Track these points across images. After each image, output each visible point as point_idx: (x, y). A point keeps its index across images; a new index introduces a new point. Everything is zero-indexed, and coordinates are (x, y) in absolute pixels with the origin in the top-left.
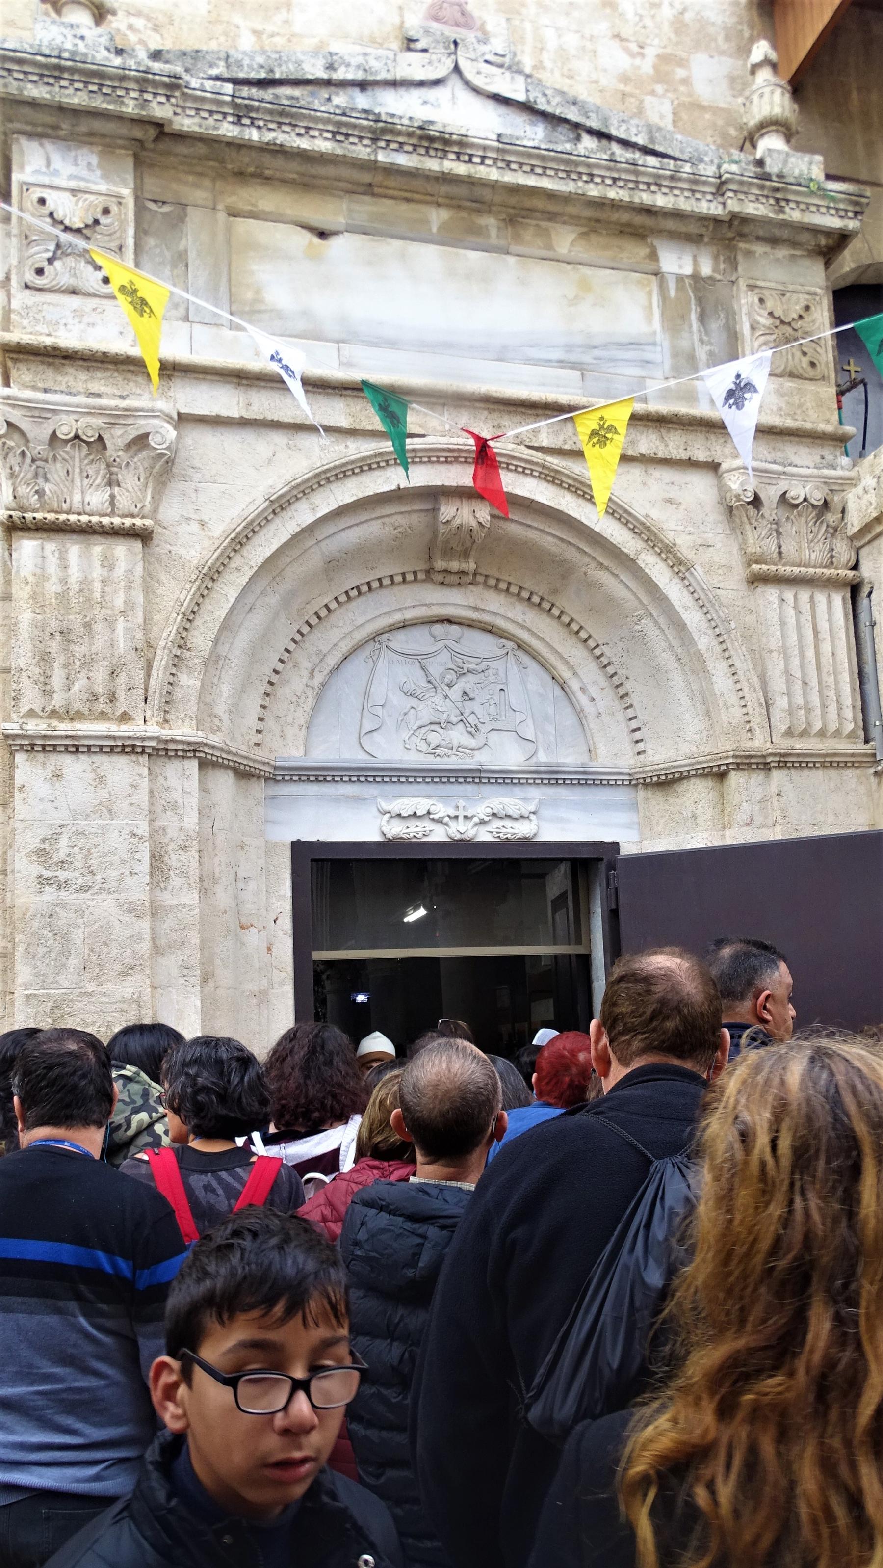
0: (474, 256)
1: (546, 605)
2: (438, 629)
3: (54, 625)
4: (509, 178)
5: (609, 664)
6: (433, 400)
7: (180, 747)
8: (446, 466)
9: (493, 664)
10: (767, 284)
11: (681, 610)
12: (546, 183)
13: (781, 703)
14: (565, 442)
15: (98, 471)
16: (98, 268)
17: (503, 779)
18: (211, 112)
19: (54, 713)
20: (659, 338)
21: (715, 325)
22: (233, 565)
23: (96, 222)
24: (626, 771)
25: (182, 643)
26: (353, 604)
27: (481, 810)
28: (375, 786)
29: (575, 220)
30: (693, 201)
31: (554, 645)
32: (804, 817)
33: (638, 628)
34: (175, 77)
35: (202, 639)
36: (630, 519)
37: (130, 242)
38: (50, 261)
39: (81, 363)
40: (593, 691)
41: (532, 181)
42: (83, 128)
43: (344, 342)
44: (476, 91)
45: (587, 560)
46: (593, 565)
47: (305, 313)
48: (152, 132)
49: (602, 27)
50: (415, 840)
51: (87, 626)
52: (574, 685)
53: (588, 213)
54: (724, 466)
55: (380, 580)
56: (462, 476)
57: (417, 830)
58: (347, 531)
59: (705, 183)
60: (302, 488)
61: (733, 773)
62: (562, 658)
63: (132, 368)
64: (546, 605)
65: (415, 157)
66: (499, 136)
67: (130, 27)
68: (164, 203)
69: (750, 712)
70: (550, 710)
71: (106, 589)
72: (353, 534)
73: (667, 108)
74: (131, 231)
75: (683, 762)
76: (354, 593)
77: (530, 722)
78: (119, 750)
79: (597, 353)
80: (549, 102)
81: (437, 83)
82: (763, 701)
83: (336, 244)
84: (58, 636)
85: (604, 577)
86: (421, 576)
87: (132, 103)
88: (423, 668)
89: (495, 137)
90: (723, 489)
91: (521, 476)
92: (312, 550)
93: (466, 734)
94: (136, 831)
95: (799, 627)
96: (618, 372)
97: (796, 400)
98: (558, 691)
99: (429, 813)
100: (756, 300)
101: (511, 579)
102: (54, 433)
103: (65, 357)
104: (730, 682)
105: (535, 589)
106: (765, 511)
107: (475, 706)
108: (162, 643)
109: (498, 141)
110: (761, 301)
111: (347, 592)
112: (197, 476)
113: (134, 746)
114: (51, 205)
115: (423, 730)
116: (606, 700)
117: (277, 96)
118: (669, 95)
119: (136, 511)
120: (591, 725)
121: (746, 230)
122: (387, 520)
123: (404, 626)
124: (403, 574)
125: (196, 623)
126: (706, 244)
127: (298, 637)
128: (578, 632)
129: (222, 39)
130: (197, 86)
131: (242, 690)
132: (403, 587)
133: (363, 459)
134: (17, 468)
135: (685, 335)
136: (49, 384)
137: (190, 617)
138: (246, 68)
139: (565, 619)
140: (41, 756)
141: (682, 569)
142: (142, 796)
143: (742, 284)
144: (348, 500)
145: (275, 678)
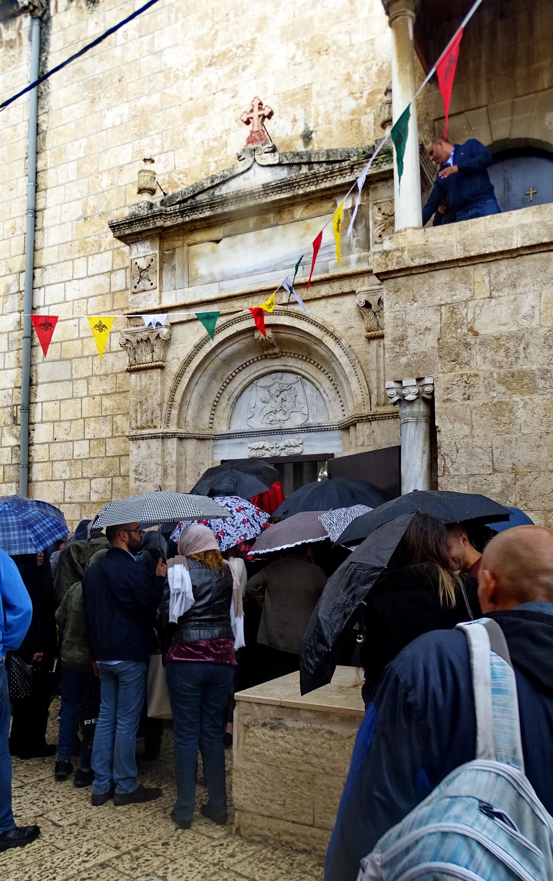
0: (266, 231)
2: (274, 375)
3: (138, 401)
9: (293, 386)
10: (383, 200)
13: (375, 392)
15: (149, 349)
16: (150, 281)
17: (290, 432)
19: (138, 428)
27: (282, 445)
29: (301, 203)
30: (342, 179)
32: (383, 441)
35: (178, 397)
37: (158, 269)
38: (138, 283)
40: (328, 391)
42: (144, 236)
47: (211, 274)
48: (161, 231)
49: (345, 92)
52: (321, 390)
53: (304, 199)
56: (251, 323)
59: (345, 169)
65: (237, 205)
67: (179, 179)
70: (315, 401)
72: (229, 350)
74: (158, 265)
76: (241, 368)
77: (306, 407)
81: (248, 169)
83: (221, 243)
85: (316, 347)
87: (151, 224)
88: (269, 391)
100: (377, 209)
104: (358, 385)
106: (373, 307)
110: (380, 209)
112: (177, 343)
116: (332, 394)
118: (373, 111)
123: (262, 376)
127: (223, 388)
131: (200, 409)
136: (138, 324)
137: (174, 391)
142: (159, 452)
143: (371, 206)
145: (215, 404)
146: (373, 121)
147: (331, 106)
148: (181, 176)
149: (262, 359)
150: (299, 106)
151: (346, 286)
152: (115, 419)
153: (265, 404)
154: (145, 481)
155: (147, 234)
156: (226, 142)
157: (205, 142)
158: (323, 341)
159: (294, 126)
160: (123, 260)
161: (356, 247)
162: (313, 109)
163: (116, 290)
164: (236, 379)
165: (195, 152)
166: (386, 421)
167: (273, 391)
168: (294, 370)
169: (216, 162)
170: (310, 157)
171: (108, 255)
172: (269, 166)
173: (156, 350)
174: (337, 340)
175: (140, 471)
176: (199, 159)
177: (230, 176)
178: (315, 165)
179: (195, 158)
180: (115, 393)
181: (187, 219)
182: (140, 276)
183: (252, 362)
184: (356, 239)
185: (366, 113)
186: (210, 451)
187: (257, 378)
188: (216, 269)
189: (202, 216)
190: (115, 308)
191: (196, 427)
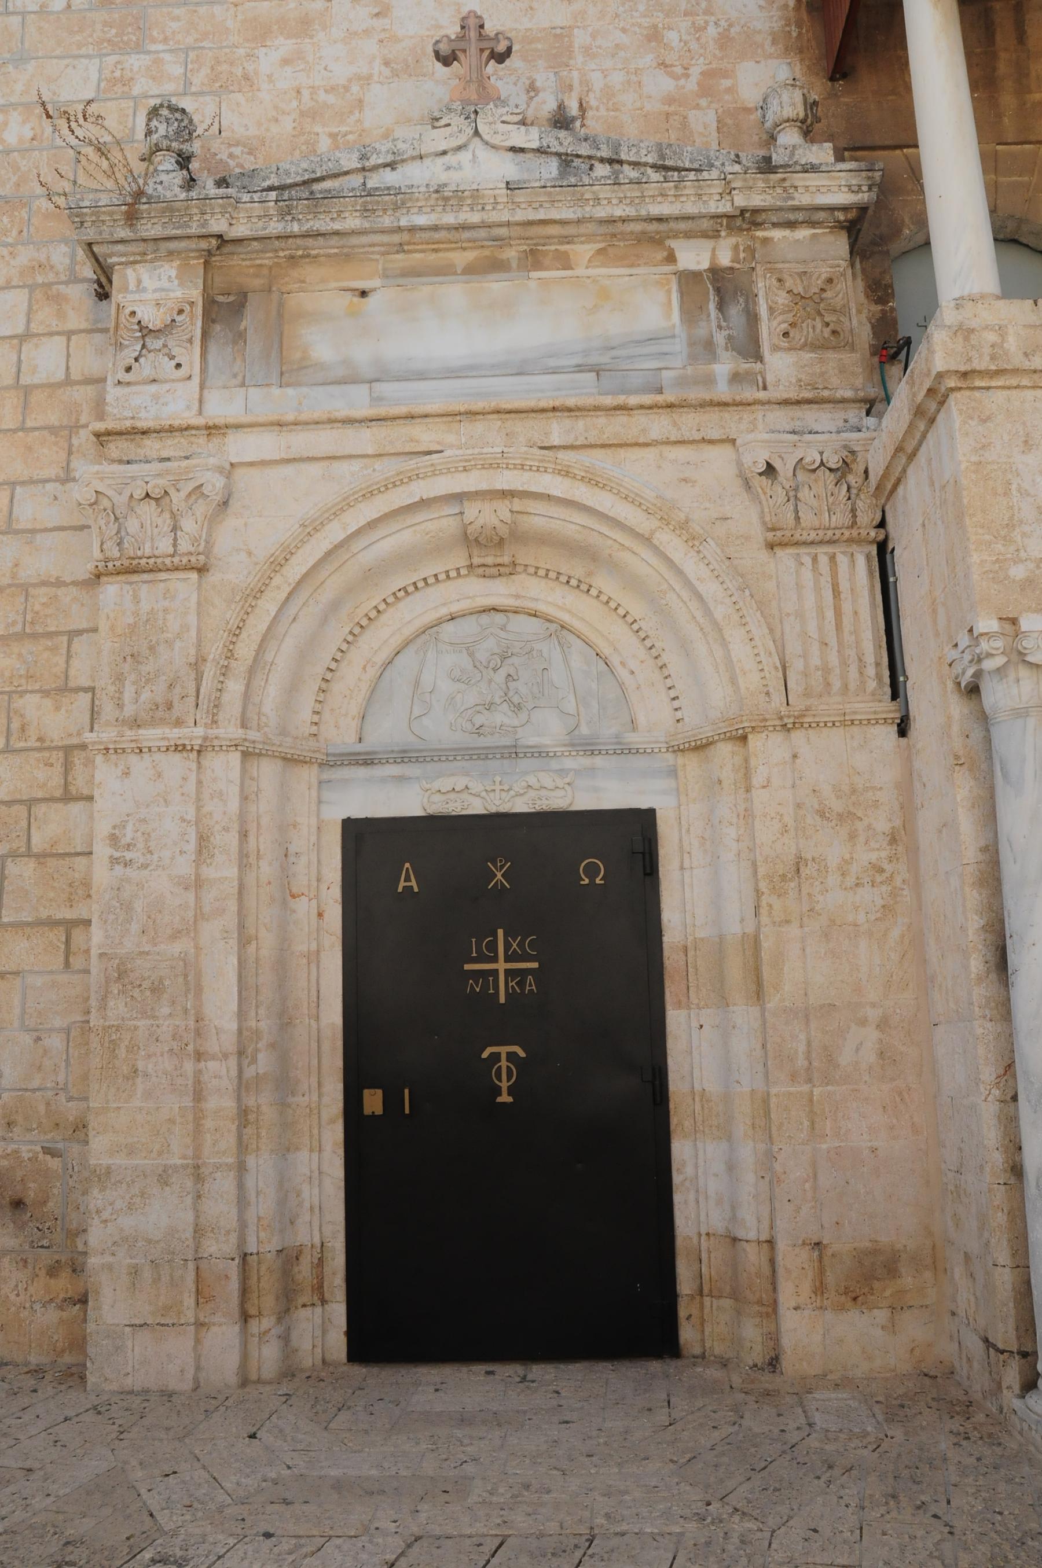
2: (485, 619)
4: (520, 216)
6: (450, 419)
7: (224, 743)
8: (465, 474)
11: (694, 582)
12: (555, 215)
13: (796, 666)
14: (576, 439)
16: (172, 358)
17: (540, 753)
18: (259, 217)
20: (678, 330)
21: (735, 311)
22: (274, 583)
23: (173, 321)
24: (662, 739)
25: (229, 654)
26: (401, 605)
28: (417, 765)
29: (590, 238)
33: (664, 602)
34: (227, 197)
35: (245, 650)
36: (642, 501)
37: (198, 332)
38: (136, 360)
39: (155, 435)
40: (633, 664)
41: (541, 215)
43: (377, 380)
44: (493, 147)
45: (610, 542)
46: (617, 546)
49: (648, 60)
50: (454, 813)
51: (152, 648)
52: (615, 661)
53: (603, 229)
54: (738, 442)
55: (425, 579)
57: (456, 805)
58: (382, 542)
60: (333, 511)
61: (750, 737)
63: (194, 432)
66: (508, 183)
67: (231, 156)
68: (229, 294)
69: (768, 675)
70: (594, 686)
71: (168, 616)
73: (711, 118)
74: (199, 323)
75: (706, 729)
76: (402, 593)
78: (173, 748)
79: (614, 353)
80: (561, 144)
81: (459, 148)
82: (778, 664)
84: (129, 658)
86: (463, 572)
88: (471, 655)
89: (504, 186)
90: (739, 464)
91: (536, 474)
94: (185, 817)
95: (818, 589)
96: (637, 367)
97: (817, 369)
99: (467, 787)
100: (775, 282)
102: (132, 496)
103: (143, 433)
106: (780, 479)
108: (211, 656)
109: (508, 189)
111: (394, 594)
113: (184, 745)
114: (139, 315)
117: (312, 193)
118: (714, 105)
119: (192, 549)
121: (759, 219)
122: (417, 528)
125: (241, 637)
126: (725, 238)
127: (350, 638)
129: (304, 147)
130: (248, 200)
133: (387, 479)
134: (104, 527)
135: (703, 324)
138: (293, 175)
140: (114, 757)
141: (697, 543)
142: (191, 787)
143: (760, 270)
144: (375, 516)
145: (329, 676)
146: (715, 125)
147: (617, 78)
148: (237, 151)
150: (541, 63)
151: (712, 423)
152: (18, 703)
154: (145, 866)
155: (173, 245)
156: (360, 101)
157: (306, 93)
158: (655, 541)
159: (531, 98)
160: (61, 315)
161: (727, 349)
162: (575, 74)
163: (36, 381)
164: (384, 618)
165: (276, 108)
166: (825, 730)
168: (542, 607)
169: (333, 136)
170: (616, 147)
171: (20, 297)
172: (513, 149)
173: (188, 525)
174: (694, 541)
175: (128, 839)
176: (287, 124)
177: (410, 153)
178: (626, 167)
179: (277, 120)
180: (21, 637)
181: (296, 228)
182: (144, 346)
183: (431, 580)
184: (725, 333)
185: (697, 107)
186: (314, 793)
187: (439, 622)
188: (362, 353)
189: (337, 226)
190: (29, 424)
191: (283, 732)
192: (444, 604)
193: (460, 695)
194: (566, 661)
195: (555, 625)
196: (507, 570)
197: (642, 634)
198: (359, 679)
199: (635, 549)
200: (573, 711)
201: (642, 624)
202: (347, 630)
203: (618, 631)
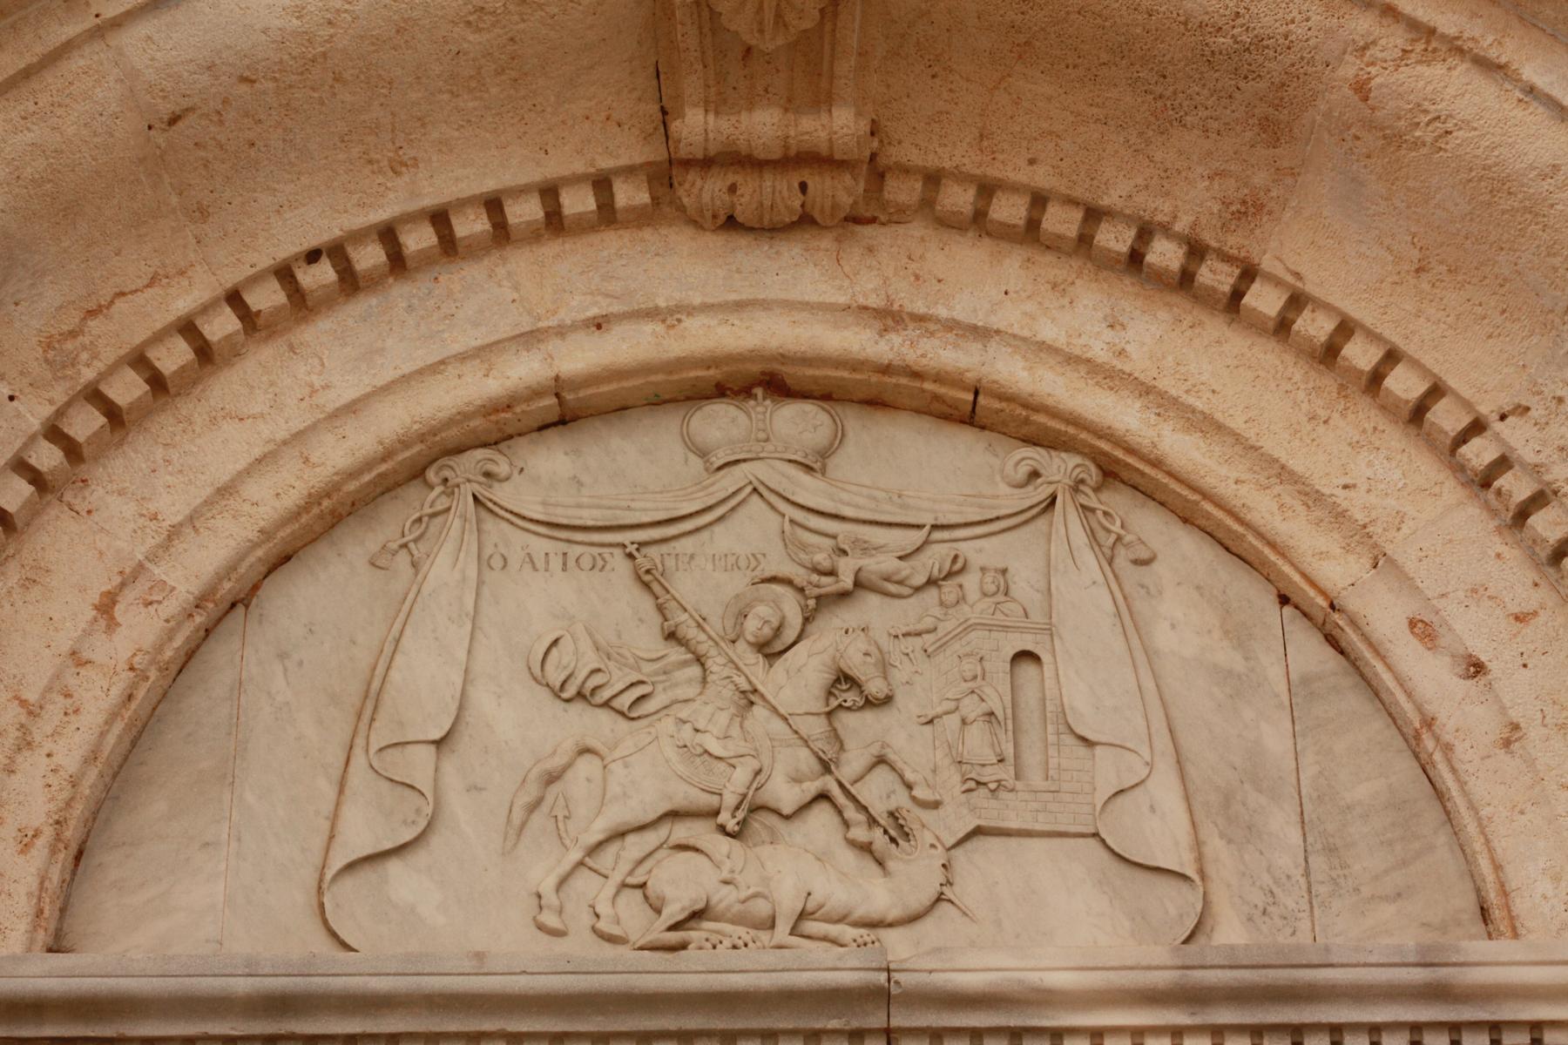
1: (1216, 276)
2: (721, 423)
5: (1539, 500)
9: (982, 552)
31: (1269, 445)
40: (1473, 629)
46: (1394, 39)
52: (1382, 614)
55: (440, 218)
62: (1312, 497)
64: (1216, 276)
70: (1275, 739)
76: (322, 275)
77: (1165, 789)
86: (628, 195)
88: (646, 581)
92: (76, 63)
93: (848, 858)
98: (1310, 653)
101: (1042, 178)
105: (1160, 209)
107: (895, 729)
111: (284, 273)
115: (635, 846)
120: (1478, 788)
123: (567, 412)
124: (549, 193)
127: (47, 457)
128: (1375, 379)
132: (551, 248)
139: (1315, 326)
149: (607, 215)
153: (597, 725)
164: (224, 387)
167: (706, 579)
168: (1011, 371)
187: (502, 427)
192: (530, 338)
193: (587, 766)
194: (1129, 619)
195: (1073, 460)
196: (837, 191)
197: (1517, 487)
198: (77, 659)
199: (1488, 44)
200: (1172, 852)
201: (1517, 436)
202: (35, 414)
203: (1387, 475)
